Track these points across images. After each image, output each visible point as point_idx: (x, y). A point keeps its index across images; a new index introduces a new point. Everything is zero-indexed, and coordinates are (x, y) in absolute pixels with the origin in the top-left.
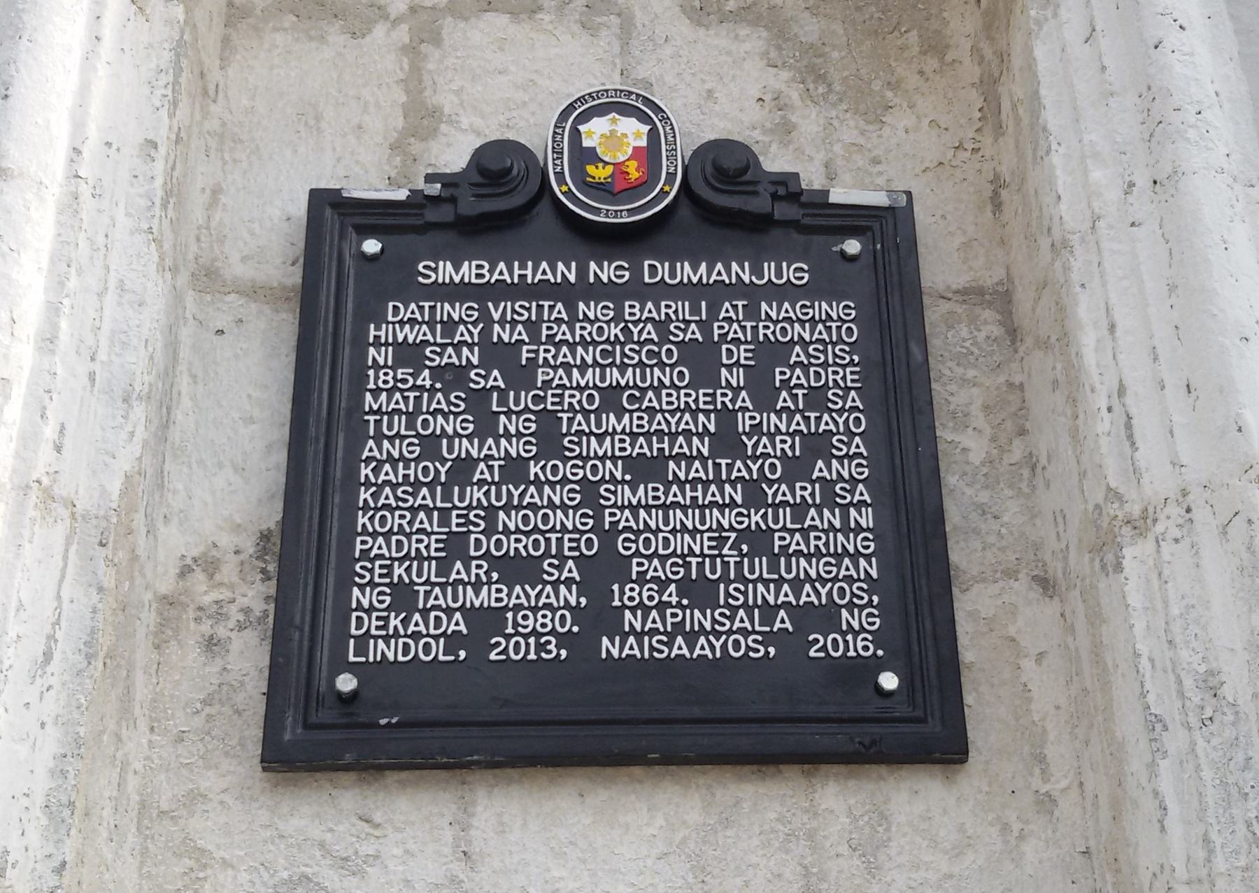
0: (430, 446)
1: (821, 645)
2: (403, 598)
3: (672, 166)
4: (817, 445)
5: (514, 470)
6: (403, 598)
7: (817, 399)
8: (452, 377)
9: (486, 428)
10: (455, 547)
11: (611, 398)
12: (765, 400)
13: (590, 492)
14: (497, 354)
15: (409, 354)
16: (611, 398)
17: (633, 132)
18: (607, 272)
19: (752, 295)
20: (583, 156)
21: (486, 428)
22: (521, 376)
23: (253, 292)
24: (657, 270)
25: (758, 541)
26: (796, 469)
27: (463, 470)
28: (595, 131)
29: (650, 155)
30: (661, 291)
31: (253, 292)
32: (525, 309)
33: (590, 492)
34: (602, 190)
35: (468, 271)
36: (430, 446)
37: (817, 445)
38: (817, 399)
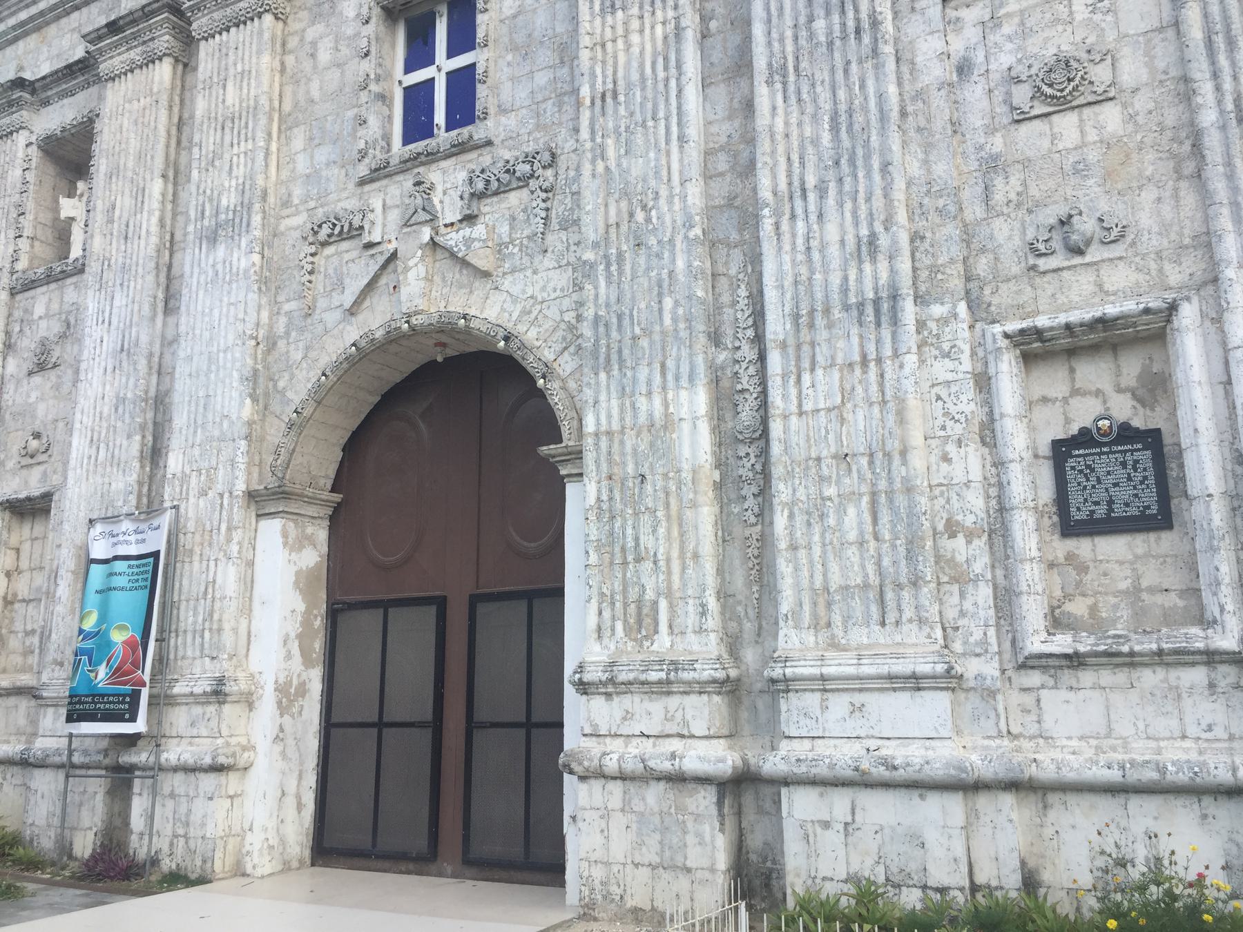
0: (1079, 484)
1: (1148, 512)
2: (1079, 509)
3: (1115, 428)
4: (1145, 478)
5: (1094, 487)
6: (1079, 509)
7: (1145, 469)
8: (1081, 471)
9: (1088, 480)
10: (1086, 500)
11: (1109, 473)
12: (1136, 471)
13: (1107, 490)
14: (1088, 467)
15: (1073, 468)
16: (1109, 473)
17: (1107, 422)
18: (1105, 449)
19: (1132, 451)
20: (1099, 429)
21: (1088, 480)
22: (1093, 470)
23: (1044, 457)
24: (1115, 448)
25: (1136, 496)
26: (1142, 483)
27: (1085, 487)
28: (1100, 423)
29: (1111, 427)
30: (1115, 452)
31: (1044, 457)
32: (1091, 458)
33: (1107, 490)
34: (1104, 435)
35: (1081, 452)
36: (1079, 484)
37: (1145, 478)
38: (1145, 469)
